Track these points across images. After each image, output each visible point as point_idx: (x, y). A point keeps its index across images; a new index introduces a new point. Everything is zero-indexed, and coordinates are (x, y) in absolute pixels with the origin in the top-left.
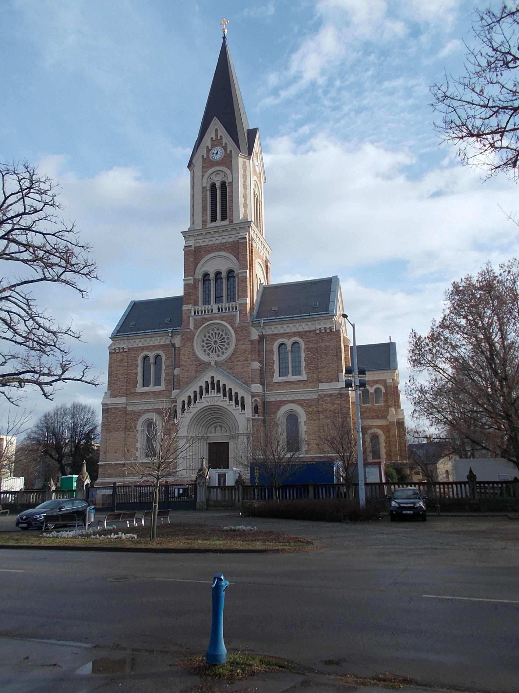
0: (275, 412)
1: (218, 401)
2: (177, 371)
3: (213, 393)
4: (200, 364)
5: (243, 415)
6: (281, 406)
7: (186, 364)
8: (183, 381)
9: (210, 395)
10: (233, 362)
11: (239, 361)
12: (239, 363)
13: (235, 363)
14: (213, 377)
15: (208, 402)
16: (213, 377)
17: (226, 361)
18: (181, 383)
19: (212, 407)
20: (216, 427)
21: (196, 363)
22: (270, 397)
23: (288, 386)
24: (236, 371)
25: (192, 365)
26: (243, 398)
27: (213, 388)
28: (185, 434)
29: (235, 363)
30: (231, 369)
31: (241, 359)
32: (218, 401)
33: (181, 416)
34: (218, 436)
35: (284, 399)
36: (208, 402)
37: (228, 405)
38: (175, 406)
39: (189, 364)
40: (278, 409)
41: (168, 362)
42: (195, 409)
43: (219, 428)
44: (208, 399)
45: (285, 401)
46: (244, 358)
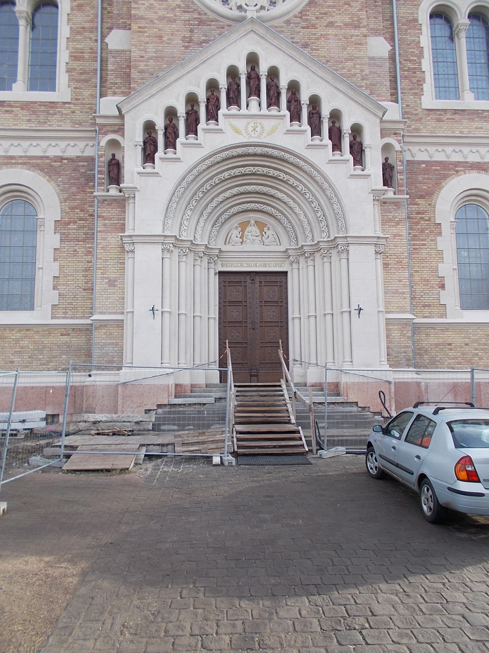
0: (428, 195)
1: (273, 131)
2: (116, 40)
3: (254, 106)
4: (201, 22)
5: (361, 182)
6: (445, 177)
7: (150, 15)
8: (142, 66)
9: (244, 111)
10: (314, 26)
11: (331, 25)
12: (331, 31)
13: (320, 31)
14: (253, 60)
15: (237, 131)
16: (253, 60)
17: (288, 22)
18: (134, 74)
19: (251, 150)
20: (244, 226)
21: (187, 16)
22: (415, 149)
23: (465, 122)
24: (322, 52)
25: (171, 21)
26: (357, 130)
27: (254, 90)
28: (158, 231)
29: (320, 31)
30: (305, 46)
31: (338, 19)
32: (273, 131)
33: (141, 170)
34: (253, 251)
35: (456, 158)
36: (237, 131)
37: (310, 147)
38: (114, 144)
39: (161, 19)
40: (438, 185)
41: (80, 18)
42: (189, 153)
43: (253, 230)
44: (240, 124)
45: (457, 164)
46: (347, 20)
